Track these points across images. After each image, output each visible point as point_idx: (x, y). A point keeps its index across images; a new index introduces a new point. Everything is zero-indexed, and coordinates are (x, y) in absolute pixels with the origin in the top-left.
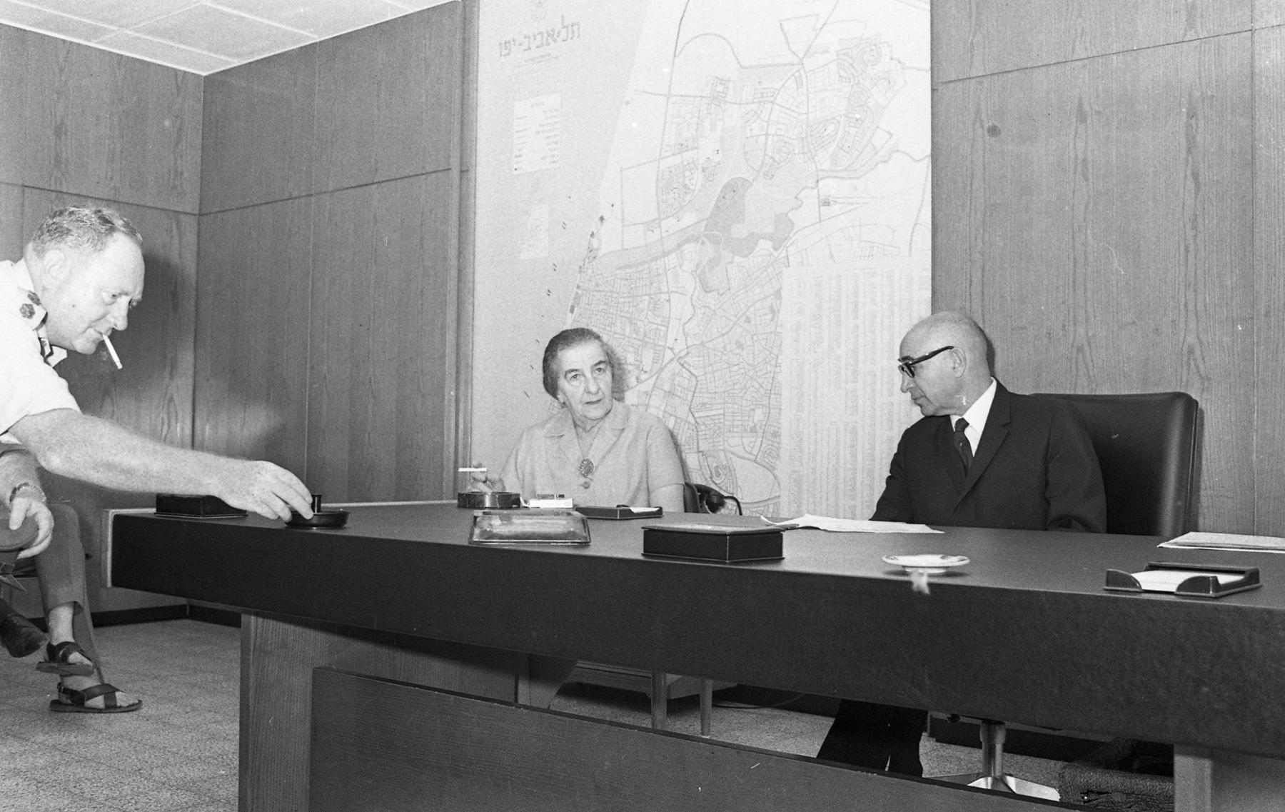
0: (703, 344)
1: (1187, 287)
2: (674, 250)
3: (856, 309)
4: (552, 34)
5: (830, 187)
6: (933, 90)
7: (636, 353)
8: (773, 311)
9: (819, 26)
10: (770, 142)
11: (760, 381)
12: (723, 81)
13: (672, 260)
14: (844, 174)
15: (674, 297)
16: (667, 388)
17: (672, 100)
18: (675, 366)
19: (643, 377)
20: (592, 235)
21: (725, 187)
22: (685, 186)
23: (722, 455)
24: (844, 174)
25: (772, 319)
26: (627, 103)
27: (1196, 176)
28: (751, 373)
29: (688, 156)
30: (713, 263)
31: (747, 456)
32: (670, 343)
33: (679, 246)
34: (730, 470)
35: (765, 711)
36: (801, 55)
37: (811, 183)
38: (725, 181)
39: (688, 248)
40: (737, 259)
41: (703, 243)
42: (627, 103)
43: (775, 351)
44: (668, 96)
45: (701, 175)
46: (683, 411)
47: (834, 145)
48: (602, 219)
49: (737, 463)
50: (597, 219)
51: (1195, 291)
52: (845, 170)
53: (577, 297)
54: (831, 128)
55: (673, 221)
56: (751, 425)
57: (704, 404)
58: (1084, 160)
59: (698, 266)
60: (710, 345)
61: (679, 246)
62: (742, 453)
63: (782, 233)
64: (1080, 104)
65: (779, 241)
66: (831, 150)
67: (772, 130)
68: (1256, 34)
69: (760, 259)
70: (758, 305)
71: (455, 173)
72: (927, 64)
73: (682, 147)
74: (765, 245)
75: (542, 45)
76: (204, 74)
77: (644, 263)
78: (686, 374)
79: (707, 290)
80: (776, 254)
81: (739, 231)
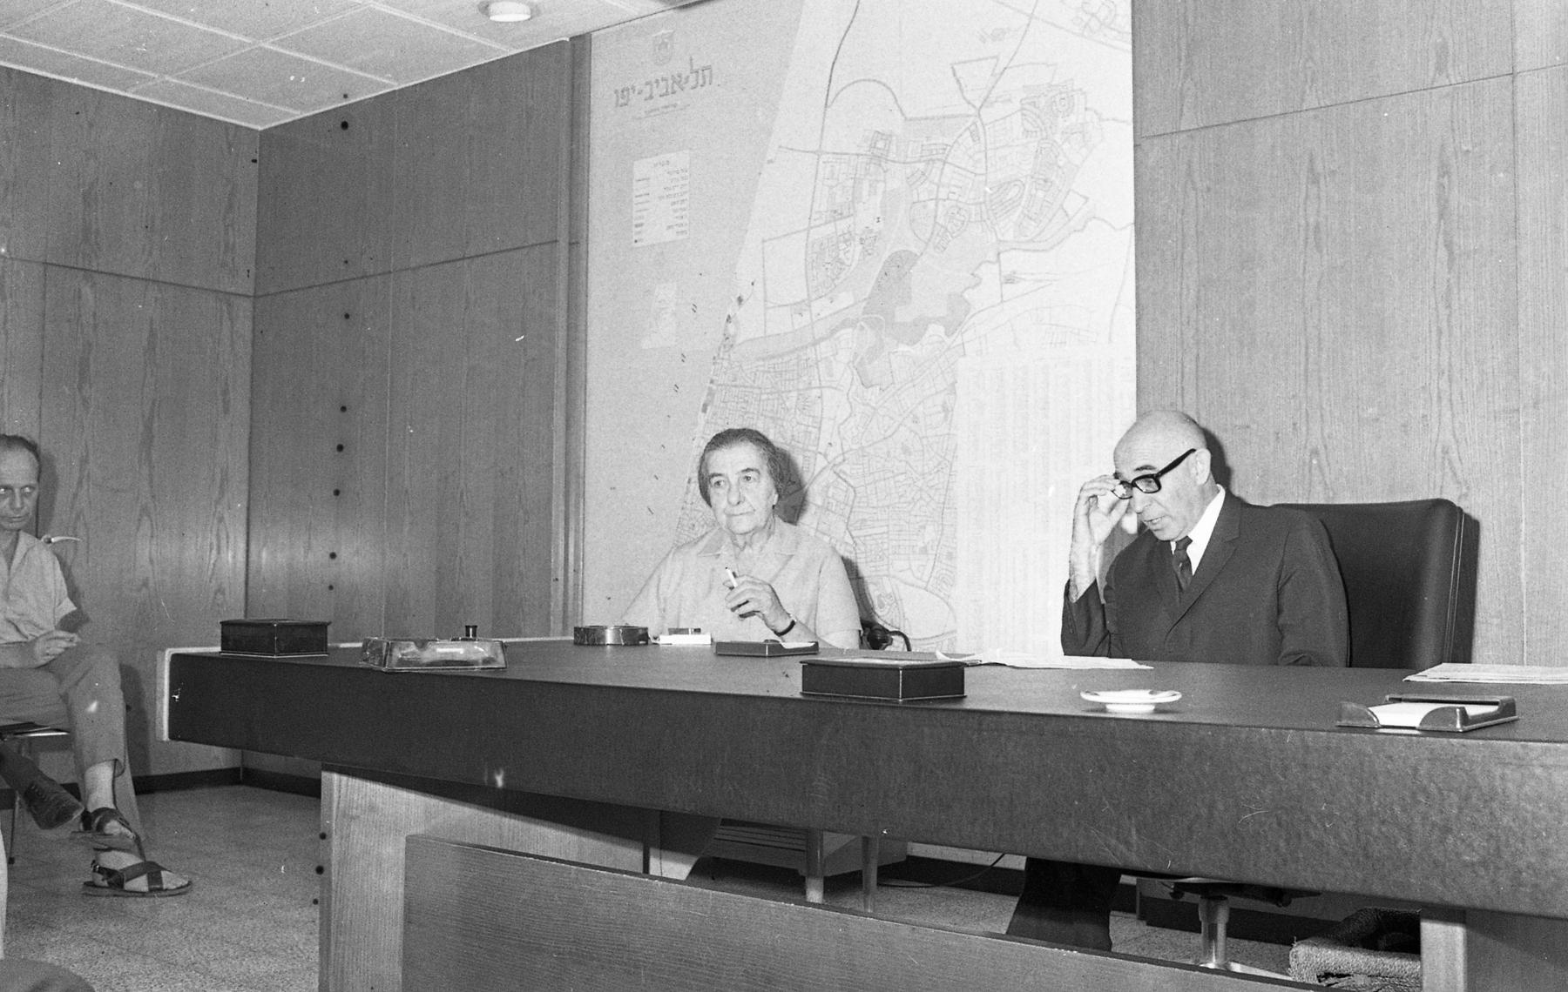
0: (862, 448)
2: (823, 339)
4: (679, 81)
6: (1135, 146)
8: (946, 409)
9: (998, 71)
10: (941, 208)
11: (932, 492)
12: (887, 137)
14: (1031, 246)
15: (827, 393)
17: (824, 158)
18: (828, 476)
24: (1031, 246)
26: (770, 162)
27: (1449, 246)
28: (919, 484)
29: (843, 225)
35: (941, 891)
36: (978, 104)
37: (992, 256)
38: (886, 255)
39: (846, 333)
40: (903, 348)
42: (770, 162)
44: (818, 153)
48: (740, 300)
50: (734, 300)
51: (1450, 380)
52: (1032, 241)
53: (711, 393)
54: (1016, 190)
55: (825, 301)
56: (921, 544)
58: (1317, 227)
60: (870, 450)
61: (833, 331)
65: (953, 327)
67: (942, 195)
68: (1519, 79)
71: (563, 244)
72: (1128, 114)
73: (837, 215)
74: (936, 330)
75: (667, 94)
76: (260, 128)
78: (843, 486)
79: (866, 385)
80: (948, 341)
81: (903, 315)
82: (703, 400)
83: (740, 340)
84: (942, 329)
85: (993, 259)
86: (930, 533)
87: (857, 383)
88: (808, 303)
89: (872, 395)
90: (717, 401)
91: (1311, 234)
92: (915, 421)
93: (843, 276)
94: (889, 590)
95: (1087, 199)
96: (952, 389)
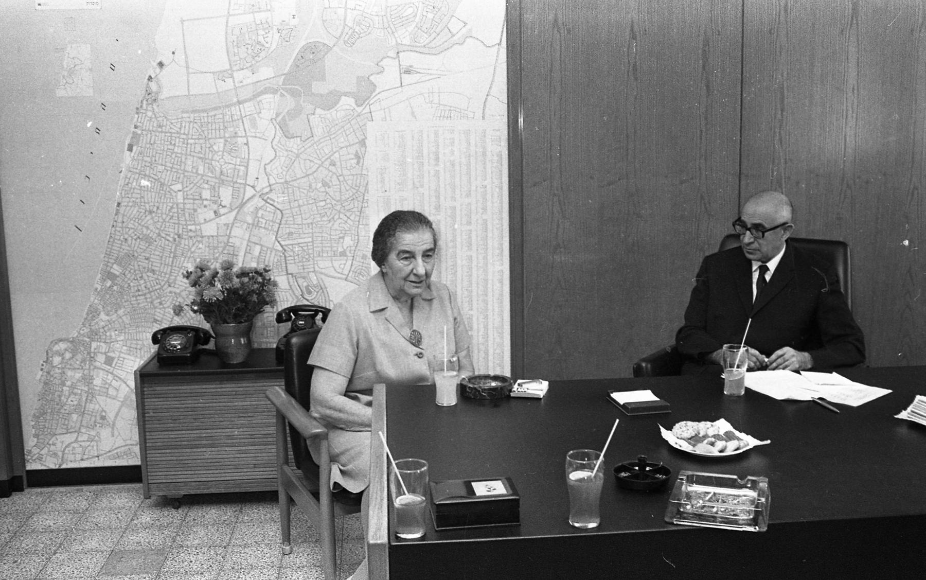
0: (286, 182)
2: (250, 100)
3: (437, 159)
5: (408, 59)
7: (213, 188)
11: (348, 214)
13: (248, 107)
19: (222, 211)
20: (150, 78)
21: (305, 48)
22: (259, 43)
23: (312, 275)
25: (358, 163)
27: (708, 87)
28: (338, 208)
30: (295, 113)
32: (250, 181)
33: (255, 96)
34: (322, 289)
37: (392, 54)
38: (303, 43)
39: (268, 97)
40: (318, 111)
41: (282, 95)
43: (362, 189)
45: (277, 36)
46: (269, 239)
47: (414, 25)
48: (161, 64)
49: (328, 281)
50: (155, 64)
55: (247, 73)
56: (340, 250)
57: (290, 234)
58: (635, 66)
59: (277, 115)
61: (255, 96)
63: (365, 92)
64: (632, 27)
65: (361, 101)
66: (410, 29)
69: (343, 113)
74: (347, 102)
79: (288, 136)
80: (359, 109)
81: (319, 88)
82: (127, 142)
83: (162, 97)
84: (351, 101)
85: (394, 55)
86: (348, 241)
87: (279, 133)
89: (294, 144)
90: (144, 141)
91: (631, 69)
92: (333, 164)
93: (263, 54)
94: (315, 282)
95: (465, 24)
96: (363, 143)
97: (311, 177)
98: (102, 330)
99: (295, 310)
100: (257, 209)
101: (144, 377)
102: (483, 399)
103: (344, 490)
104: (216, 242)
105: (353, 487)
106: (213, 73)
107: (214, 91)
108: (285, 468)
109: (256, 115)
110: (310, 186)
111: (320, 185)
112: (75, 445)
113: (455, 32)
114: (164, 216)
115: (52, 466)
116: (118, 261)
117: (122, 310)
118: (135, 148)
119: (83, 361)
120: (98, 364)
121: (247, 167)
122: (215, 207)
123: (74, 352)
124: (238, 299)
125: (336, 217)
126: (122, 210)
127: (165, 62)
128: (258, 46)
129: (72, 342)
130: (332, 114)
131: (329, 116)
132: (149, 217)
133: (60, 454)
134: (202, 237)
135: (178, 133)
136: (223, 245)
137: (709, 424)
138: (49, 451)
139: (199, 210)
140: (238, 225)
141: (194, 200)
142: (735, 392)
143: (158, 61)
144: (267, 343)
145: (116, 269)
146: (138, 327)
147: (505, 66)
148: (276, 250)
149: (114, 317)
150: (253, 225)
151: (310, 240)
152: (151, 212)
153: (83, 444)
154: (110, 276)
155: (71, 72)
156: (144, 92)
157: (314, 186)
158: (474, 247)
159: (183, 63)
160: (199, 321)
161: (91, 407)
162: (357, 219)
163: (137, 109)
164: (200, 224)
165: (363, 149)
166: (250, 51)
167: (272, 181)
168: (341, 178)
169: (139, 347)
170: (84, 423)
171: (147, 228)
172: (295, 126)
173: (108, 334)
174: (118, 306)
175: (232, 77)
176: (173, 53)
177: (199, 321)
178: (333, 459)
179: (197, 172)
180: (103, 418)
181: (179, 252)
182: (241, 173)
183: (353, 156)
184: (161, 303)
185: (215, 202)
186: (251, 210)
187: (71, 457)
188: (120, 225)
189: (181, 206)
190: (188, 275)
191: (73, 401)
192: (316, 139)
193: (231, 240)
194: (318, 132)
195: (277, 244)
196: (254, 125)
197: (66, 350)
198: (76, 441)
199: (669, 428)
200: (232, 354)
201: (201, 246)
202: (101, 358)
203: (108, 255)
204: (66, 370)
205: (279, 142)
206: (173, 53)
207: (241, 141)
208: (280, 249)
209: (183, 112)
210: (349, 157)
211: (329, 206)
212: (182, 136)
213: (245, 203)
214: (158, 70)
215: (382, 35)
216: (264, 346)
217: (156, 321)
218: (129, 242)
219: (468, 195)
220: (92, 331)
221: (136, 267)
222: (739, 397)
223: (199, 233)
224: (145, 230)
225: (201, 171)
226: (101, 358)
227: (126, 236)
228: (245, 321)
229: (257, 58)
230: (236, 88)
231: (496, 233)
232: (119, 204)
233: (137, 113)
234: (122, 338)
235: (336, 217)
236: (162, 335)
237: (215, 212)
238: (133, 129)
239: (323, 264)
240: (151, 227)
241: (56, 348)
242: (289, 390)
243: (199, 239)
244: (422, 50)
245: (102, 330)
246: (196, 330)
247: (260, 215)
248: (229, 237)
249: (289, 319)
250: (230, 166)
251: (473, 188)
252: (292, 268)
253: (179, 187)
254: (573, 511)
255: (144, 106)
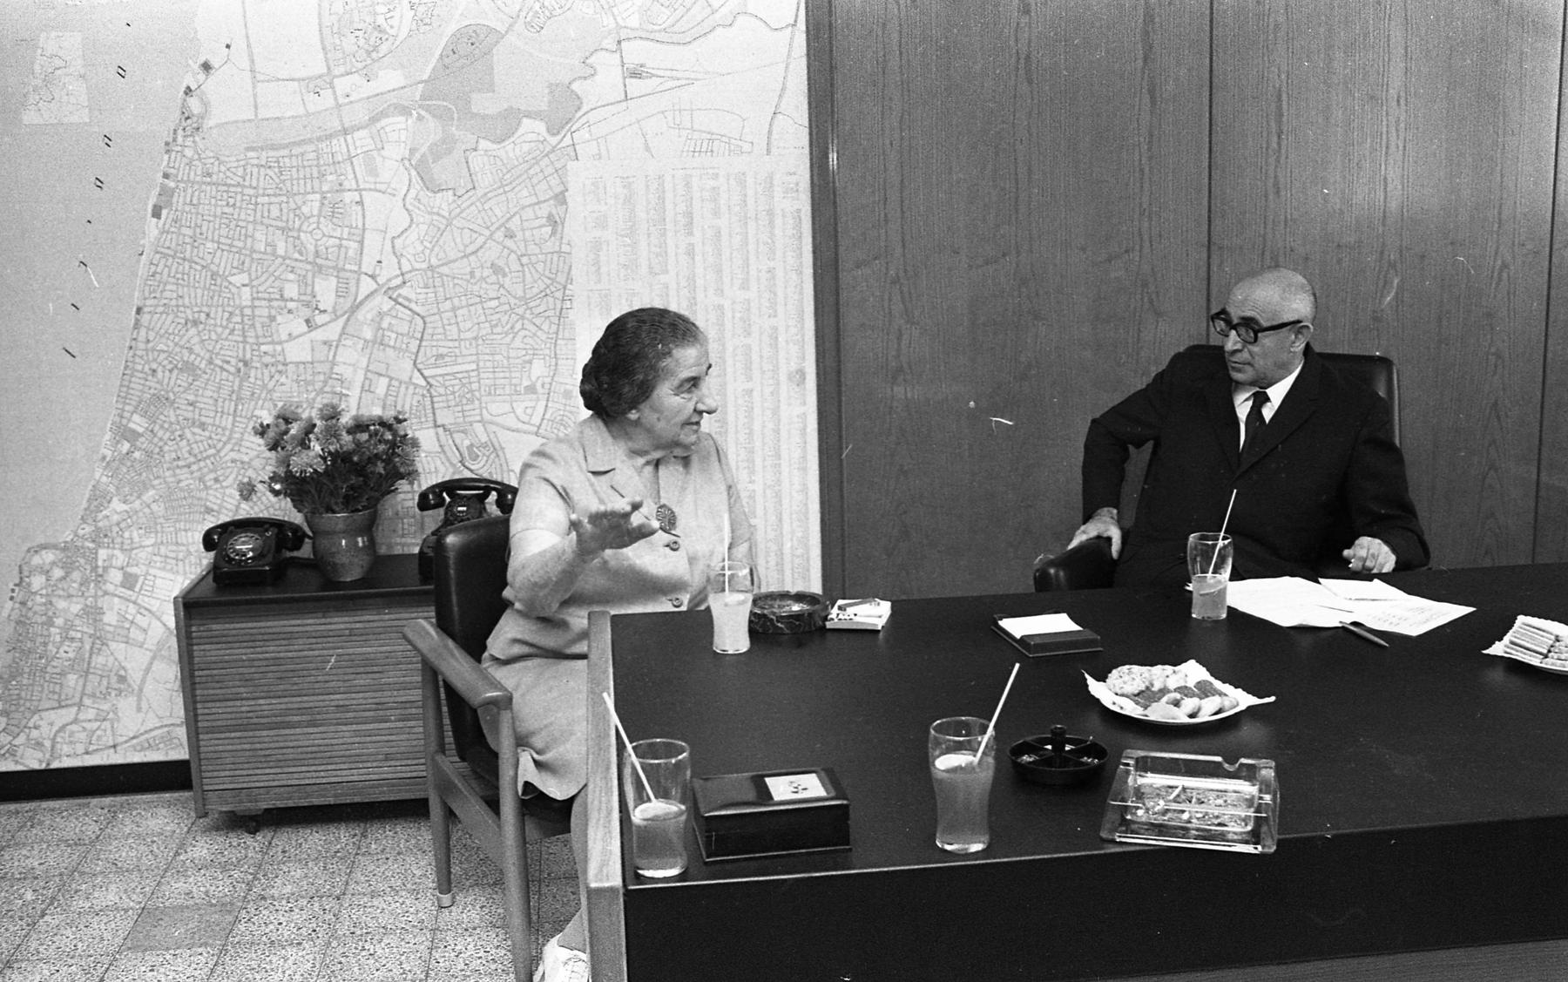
1: (1142, 214)
5: (635, 53)
7: (303, 281)
8: (554, 223)
11: (538, 321)
13: (362, 139)
16: (368, 334)
19: (320, 319)
21: (457, 36)
22: (378, 28)
25: (554, 233)
27: (1152, 92)
28: (520, 311)
30: (443, 149)
31: (526, 427)
32: (367, 267)
33: (374, 120)
34: (496, 450)
38: (452, 28)
39: (397, 121)
40: (483, 144)
41: (420, 118)
46: (404, 368)
48: (206, 67)
49: (505, 437)
53: (166, 193)
56: (526, 383)
57: (442, 356)
58: (1028, 58)
59: (412, 151)
60: (445, 270)
61: (374, 120)
62: (511, 421)
63: (563, 110)
69: (526, 147)
70: (529, 213)
74: (532, 129)
77: (310, 141)
80: (554, 140)
81: (483, 104)
84: (540, 127)
86: (538, 369)
88: (329, 79)
89: (443, 201)
90: (178, 200)
93: (384, 48)
94: (484, 439)
96: (561, 198)
97: (472, 258)
98: (116, 529)
99: (451, 487)
100: (381, 315)
101: (191, 607)
102: (778, 633)
103: (542, 797)
104: (310, 371)
105: (556, 790)
106: (299, 80)
107: (301, 111)
108: (439, 758)
109: (375, 153)
110: (472, 273)
111: (487, 272)
112: (74, 727)
113: (716, 5)
114: (219, 330)
115: (36, 766)
116: (142, 409)
117: (152, 492)
118: (164, 212)
119: (84, 583)
120: (110, 588)
121: (361, 243)
122: (307, 312)
123: (68, 567)
124: (353, 468)
125: (518, 326)
126: (145, 318)
127: (215, 63)
128: (376, 34)
129: (65, 549)
130: (512, 151)
131: (502, 153)
132: (193, 331)
133: (48, 744)
134: (285, 364)
135: (239, 184)
136: (322, 377)
137: (1169, 668)
138: (28, 739)
139: (279, 319)
140: (348, 342)
141: (270, 300)
142: (1211, 614)
143: (202, 60)
144: (403, 545)
145: (138, 423)
146: (178, 521)
147: (804, 62)
148: (416, 386)
149: (137, 505)
150: (374, 342)
151: (474, 366)
152: (196, 323)
153: (88, 726)
154: (132, 436)
155: (48, 81)
156: (178, 113)
157: (478, 275)
158: (756, 374)
159: (246, 64)
160: (283, 509)
161: (99, 660)
162: (554, 327)
163: (167, 144)
164: (280, 343)
165: (562, 209)
166: (362, 42)
167: (406, 267)
168: (525, 260)
169: (181, 556)
170: (89, 690)
171: (191, 350)
172: (444, 171)
173: (127, 535)
174: (146, 487)
175: (333, 88)
176: (228, 46)
177: (283, 509)
178: (522, 742)
179: (274, 254)
180: (122, 679)
181: (246, 393)
182: (351, 253)
183: (544, 221)
184: (216, 480)
185: (307, 305)
186: (369, 316)
187: (66, 749)
188: (142, 346)
189: (248, 311)
190: (262, 431)
191: (69, 650)
192: (480, 192)
193: (336, 369)
194: (485, 181)
195: (417, 374)
196: (373, 171)
197: (53, 563)
198: (75, 721)
199: (1101, 677)
200: (343, 565)
201: (283, 379)
202: (115, 576)
203: (123, 399)
204: (54, 600)
205: (417, 199)
206: (228, 46)
207: (349, 197)
208: (424, 383)
209: (248, 149)
210: (537, 223)
211: (507, 307)
212: (247, 191)
213: (361, 303)
214: (202, 77)
215: (591, 11)
216: (398, 550)
217: (209, 511)
218: (160, 374)
219: (745, 286)
220: (98, 530)
221: (173, 419)
222: (1217, 622)
223: (280, 358)
224: (185, 352)
225: (281, 252)
226: (115, 576)
227: (154, 366)
228: (365, 508)
229: (374, 55)
230: (339, 106)
231: (794, 349)
232: (139, 311)
233: (168, 152)
234: (152, 541)
235: (518, 326)
236: (220, 535)
237: (307, 321)
238: (161, 180)
239: (494, 408)
240: (197, 348)
241: (36, 560)
242: (444, 625)
243: (280, 367)
244: (658, 36)
245: (116, 529)
246: (279, 525)
247: (385, 325)
248: (333, 364)
249: (441, 503)
250: (332, 241)
251: (753, 272)
252: (444, 417)
253: (244, 278)
254: (939, 829)
255: (180, 139)
